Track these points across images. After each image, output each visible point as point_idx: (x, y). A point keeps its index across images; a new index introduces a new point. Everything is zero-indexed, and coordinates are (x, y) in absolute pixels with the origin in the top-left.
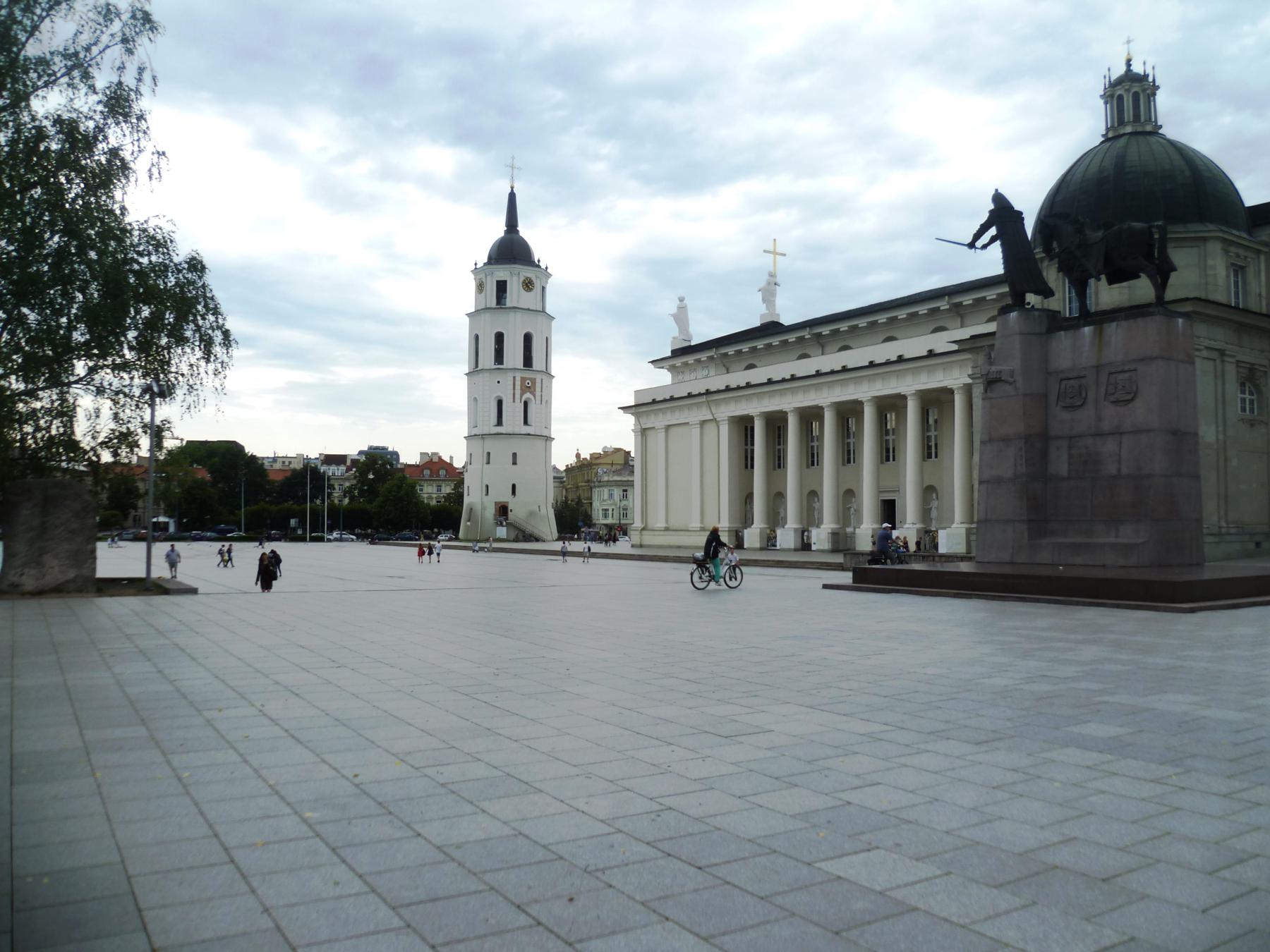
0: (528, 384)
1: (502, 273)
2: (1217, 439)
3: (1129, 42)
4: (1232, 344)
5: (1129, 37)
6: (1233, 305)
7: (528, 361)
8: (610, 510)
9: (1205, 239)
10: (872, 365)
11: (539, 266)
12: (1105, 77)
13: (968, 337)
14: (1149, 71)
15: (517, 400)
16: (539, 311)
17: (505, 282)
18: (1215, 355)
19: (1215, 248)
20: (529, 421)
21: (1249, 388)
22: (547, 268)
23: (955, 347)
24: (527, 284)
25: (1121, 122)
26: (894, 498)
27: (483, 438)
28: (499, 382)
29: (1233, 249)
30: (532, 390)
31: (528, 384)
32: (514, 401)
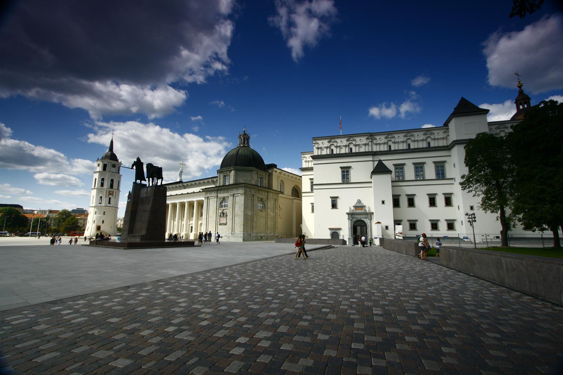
2: (251, 214)
7: (112, 186)
9: (252, 171)
10: (188, 193)
18: (252, 196)
22: (121, 162)
29: (259, 173)
32: (106, 197)
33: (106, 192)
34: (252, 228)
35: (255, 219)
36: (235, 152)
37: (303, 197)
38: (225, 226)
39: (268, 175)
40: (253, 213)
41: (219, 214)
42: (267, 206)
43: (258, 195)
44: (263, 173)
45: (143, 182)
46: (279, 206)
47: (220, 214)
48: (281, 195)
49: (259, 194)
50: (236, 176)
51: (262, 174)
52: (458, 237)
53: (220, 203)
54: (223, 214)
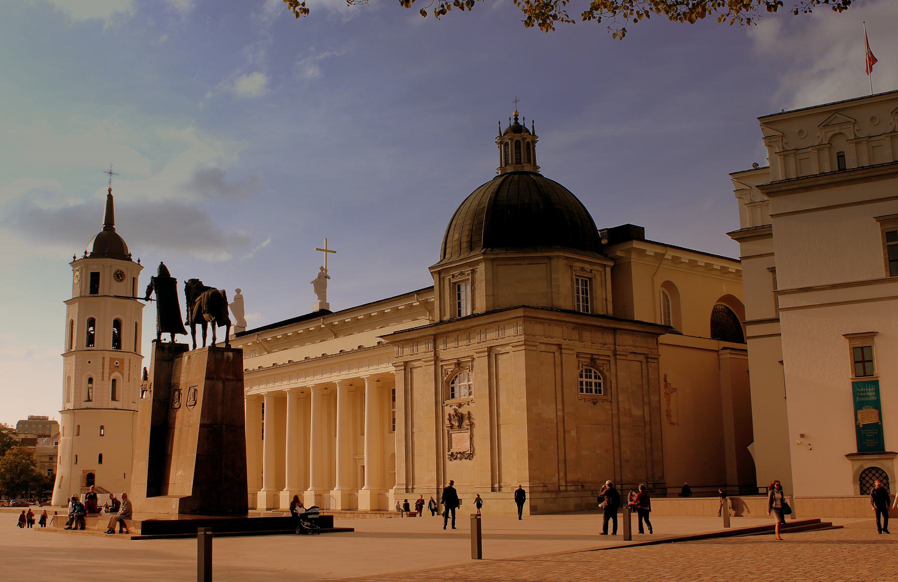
0: (117, 363)
2: (557, 415)
3: (516, 102)
15: (106, 378)
16: (129, 298)
17: (98, 273)
18: (554, 348)
20: (117, 399)
21: (595, 373)
22: (139, 261)
24: (118, 277)
25: (506, 164)
27: (74, 413)
28: (89, 362)
29: (578, 265)
30: (120, 369)
31: (117, 363)
32: (103, 380)
33: (101, 363)
34: (562, 466)
35: (573, 433)
38: (468, 461)
39: (613, 269)
40: (563, 410)
41: (447, 422)
42: (614, 381)
43: (577, 343)
44: (591, 263)
45: (180, 339)
46: (665, 380)
47: (450, 420)
48: (665, 338)
49: (580, 339)
50: (493, 282)
51: (587, 267)
52: (681, 489)
53: (447, 382)
54: (461, 420)
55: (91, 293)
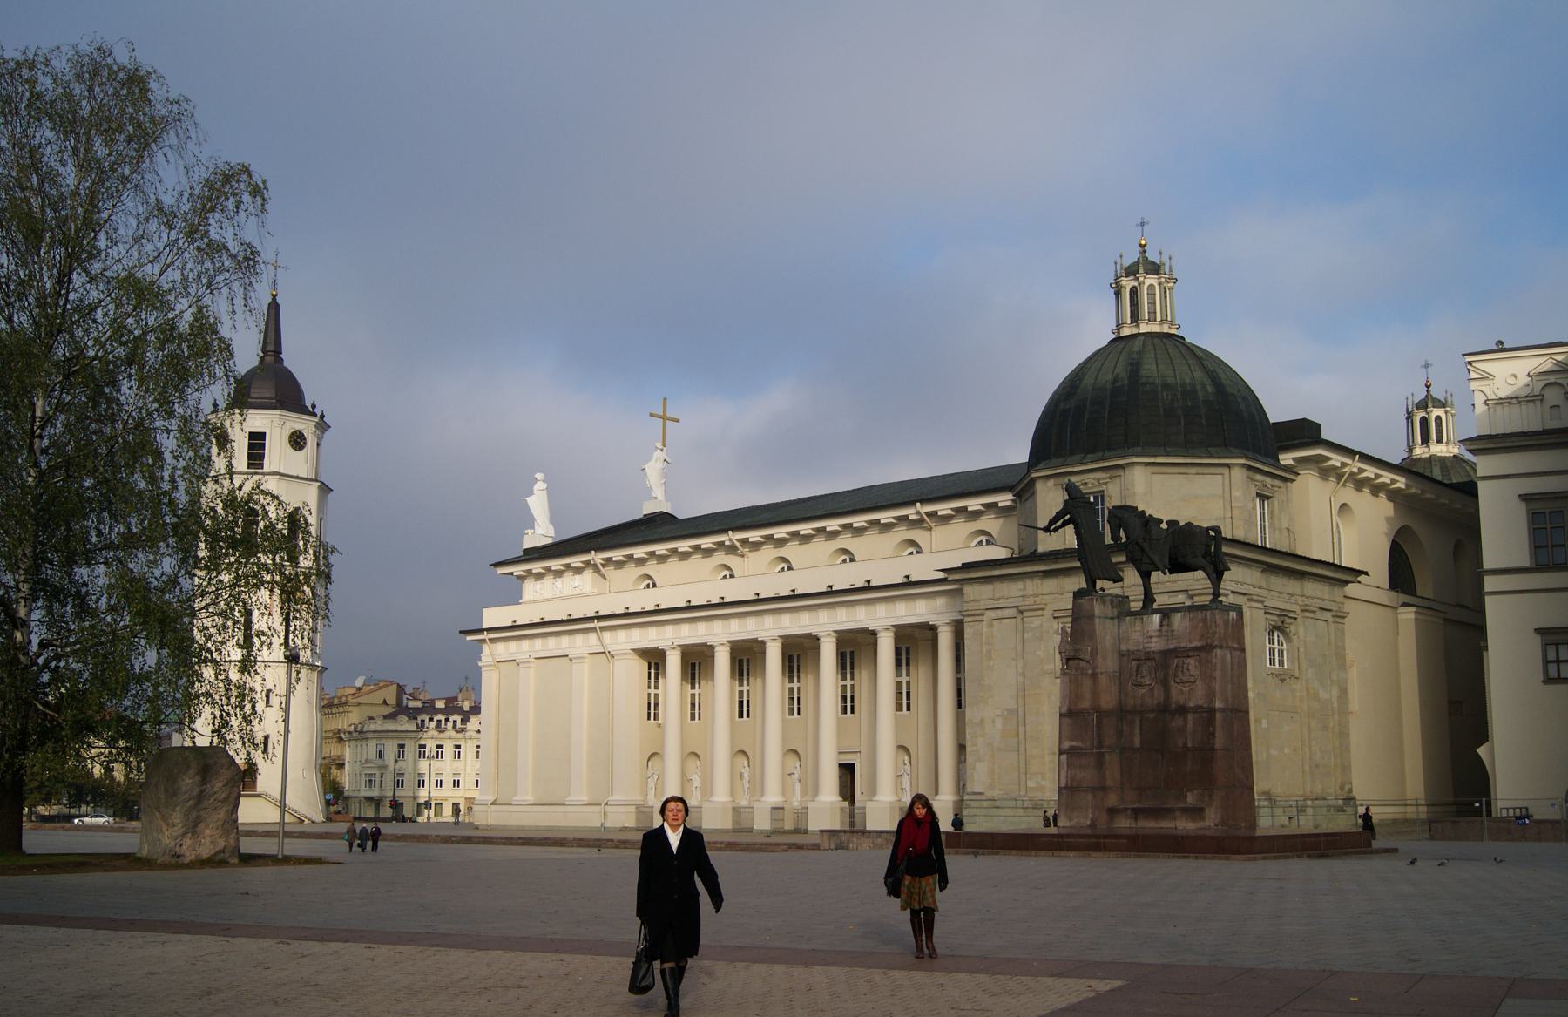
1: (258, 420)
3: (1142, 224)
4: (1260, 588)
5: (1142, 219)
6: (1260, 544)
8: (378, 776)
11: (315, 415)
12: (1116, 263)
13: (960, 565)
14: (1165, 259)
16: (311, 480)
17: (262, 436)
19: (1238, 474)
21: (1278, 636)
23: (941, 575)
24: (298, 444)
26: (852, 762)
29: (1259, 477)
36: (1122, 371)
37: (1488, 599)
55: (248, 468)
